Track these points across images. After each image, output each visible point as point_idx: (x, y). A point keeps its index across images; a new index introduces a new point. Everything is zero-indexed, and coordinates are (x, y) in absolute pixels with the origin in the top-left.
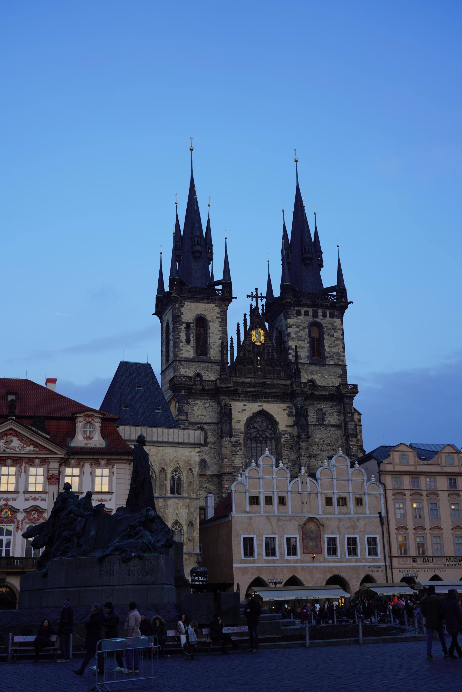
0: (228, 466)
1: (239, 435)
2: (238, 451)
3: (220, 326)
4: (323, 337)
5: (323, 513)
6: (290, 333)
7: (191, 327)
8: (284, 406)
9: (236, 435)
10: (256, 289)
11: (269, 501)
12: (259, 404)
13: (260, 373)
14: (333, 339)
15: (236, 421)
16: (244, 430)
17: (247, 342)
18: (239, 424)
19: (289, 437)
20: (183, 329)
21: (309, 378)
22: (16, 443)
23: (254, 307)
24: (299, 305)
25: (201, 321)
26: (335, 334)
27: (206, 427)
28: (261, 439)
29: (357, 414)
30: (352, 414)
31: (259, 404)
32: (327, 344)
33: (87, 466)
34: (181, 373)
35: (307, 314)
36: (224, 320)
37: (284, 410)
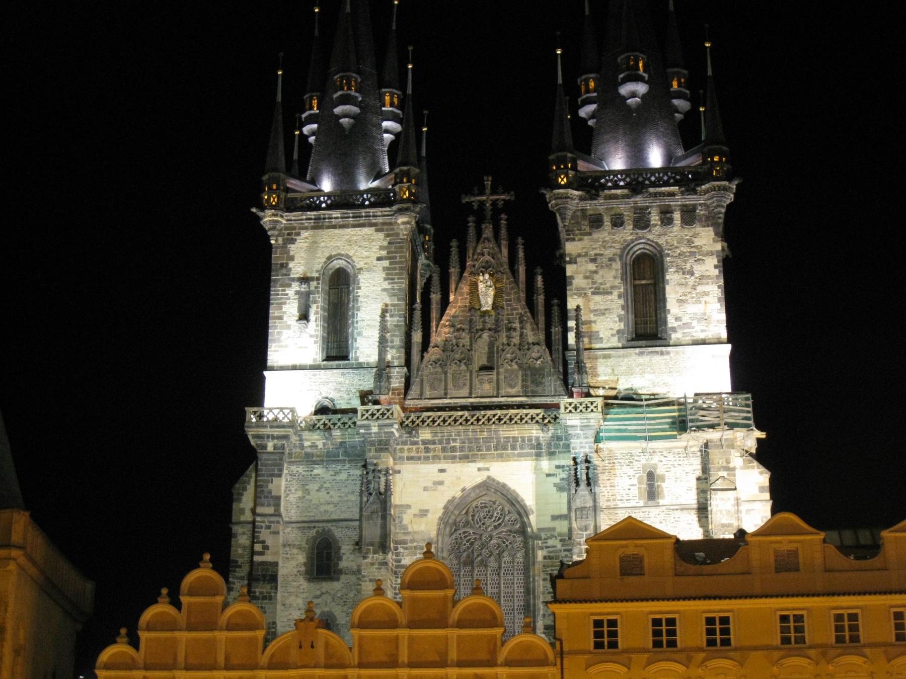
3: (385, 279)
4: (663, 277)
9: (416, 548)
12: (481, 465)
13: (487, 387)
14: (691, 280)
15: (417, 512)
16: (438, 535)
18: (424, 519)
19: (559, 546)
30: (731, 470)
35: (618, 222)
37: (548, 475)
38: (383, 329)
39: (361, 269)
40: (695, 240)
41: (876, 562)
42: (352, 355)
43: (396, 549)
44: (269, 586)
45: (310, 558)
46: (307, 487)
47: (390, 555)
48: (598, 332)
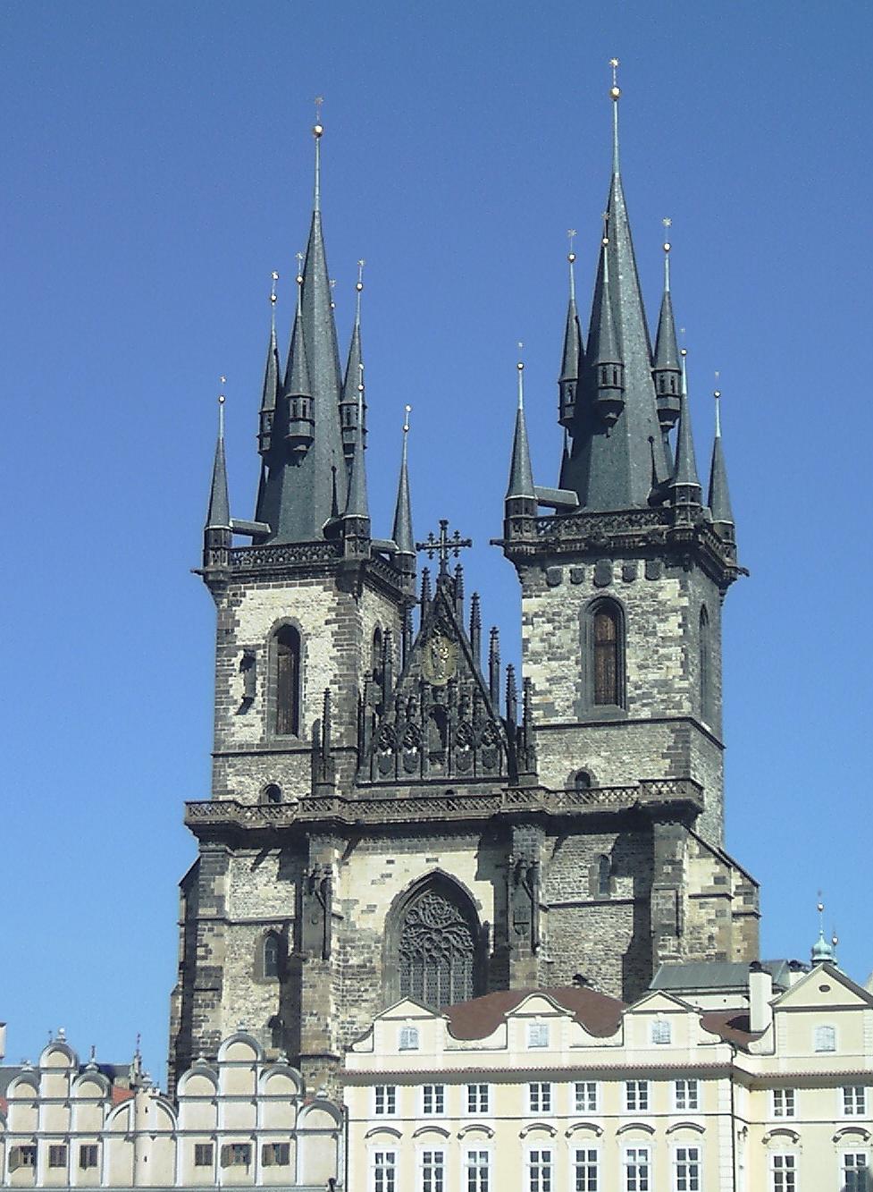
0: (316, 1036)
1: (369, 947)
2: (366, 990)
3: (334, 646)
6: (527, 641)
7: (259, 657)
9: (363, 947)
10: (444, 523)
11: (58, 1157)
12: (429, 855)
13: (439, 766)
15: (365, 908)
20: (237, 666)
21: (576, 768)
23: (433, 576)
25: (288, 637)
26: (661, 627)
29: (713, 860)
30: (677, 865)
31: (429, 855)
32: (631, 661)
34: (230, 788)
35: (576, 580)
36: (345, 627)
37: (497, 866)
39: (309, 634)
40: (660, 594)
41: (617, 1038)
42: (300, 732)
43: (344, 948)
44: (210, 994)
46: (255, 882)
48: (553, 703)
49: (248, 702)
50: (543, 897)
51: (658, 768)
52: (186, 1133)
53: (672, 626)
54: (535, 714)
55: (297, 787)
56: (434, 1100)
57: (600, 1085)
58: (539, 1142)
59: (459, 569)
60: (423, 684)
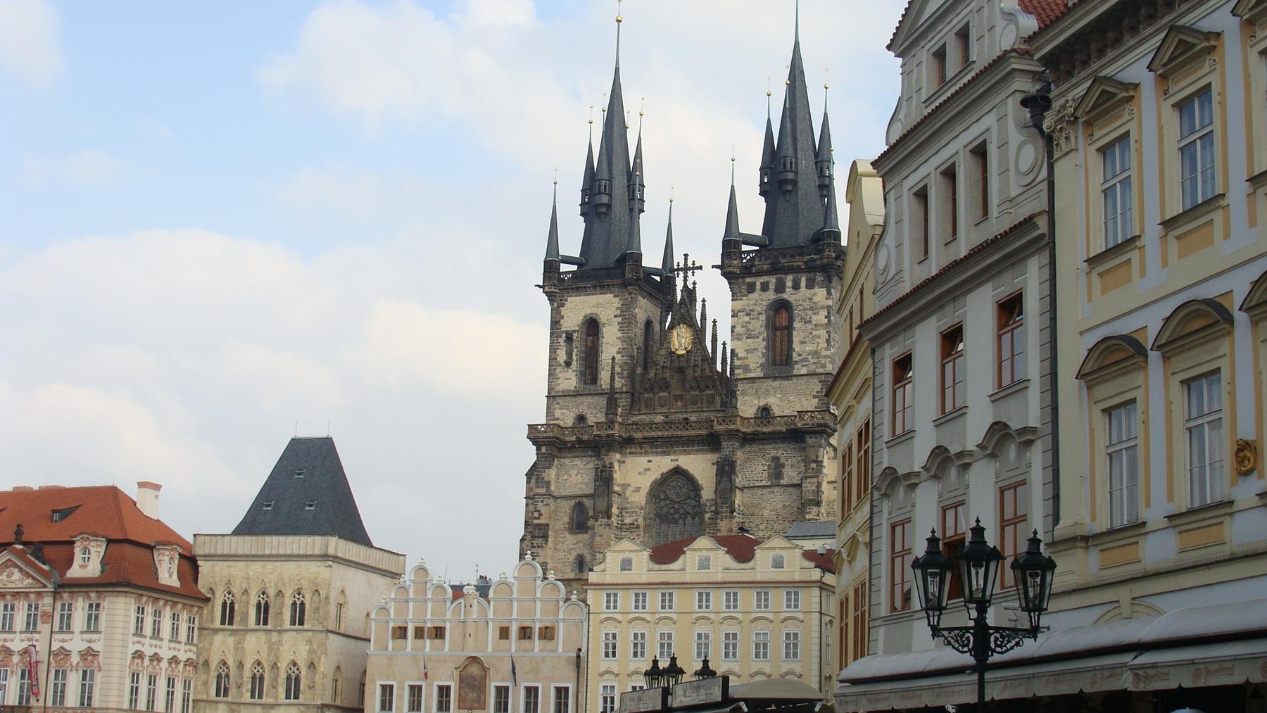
5: (494, 649)
8: (713, 457)
10: (686, 255)
11: (419, 633)
13: (679, 403)
14: (809, 326)
17: (663, 352)
20: (562, 343)
22: (17, 575)
24: (751, 275)
26: (814, 318)
27: (588, 503)
28: (677, 516)
30: (819, 463)
33: (80, 599)
35: (765, 287)
38: (613, 368)
41: (751, 564)
45: (572, 519)
47: (614, 519)
49: (568, 364)
50: (739, 481)
51: (811, 404)
52: (493, 620)
53: (821, 317)
54: (737, 371)
55: (595, 416)
56: (640, 601)
57: (740, 593)
58: (703, 628)
59: (694, 283)
60: (672, 353)
